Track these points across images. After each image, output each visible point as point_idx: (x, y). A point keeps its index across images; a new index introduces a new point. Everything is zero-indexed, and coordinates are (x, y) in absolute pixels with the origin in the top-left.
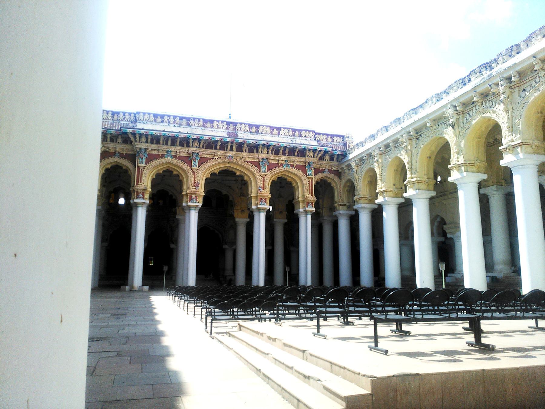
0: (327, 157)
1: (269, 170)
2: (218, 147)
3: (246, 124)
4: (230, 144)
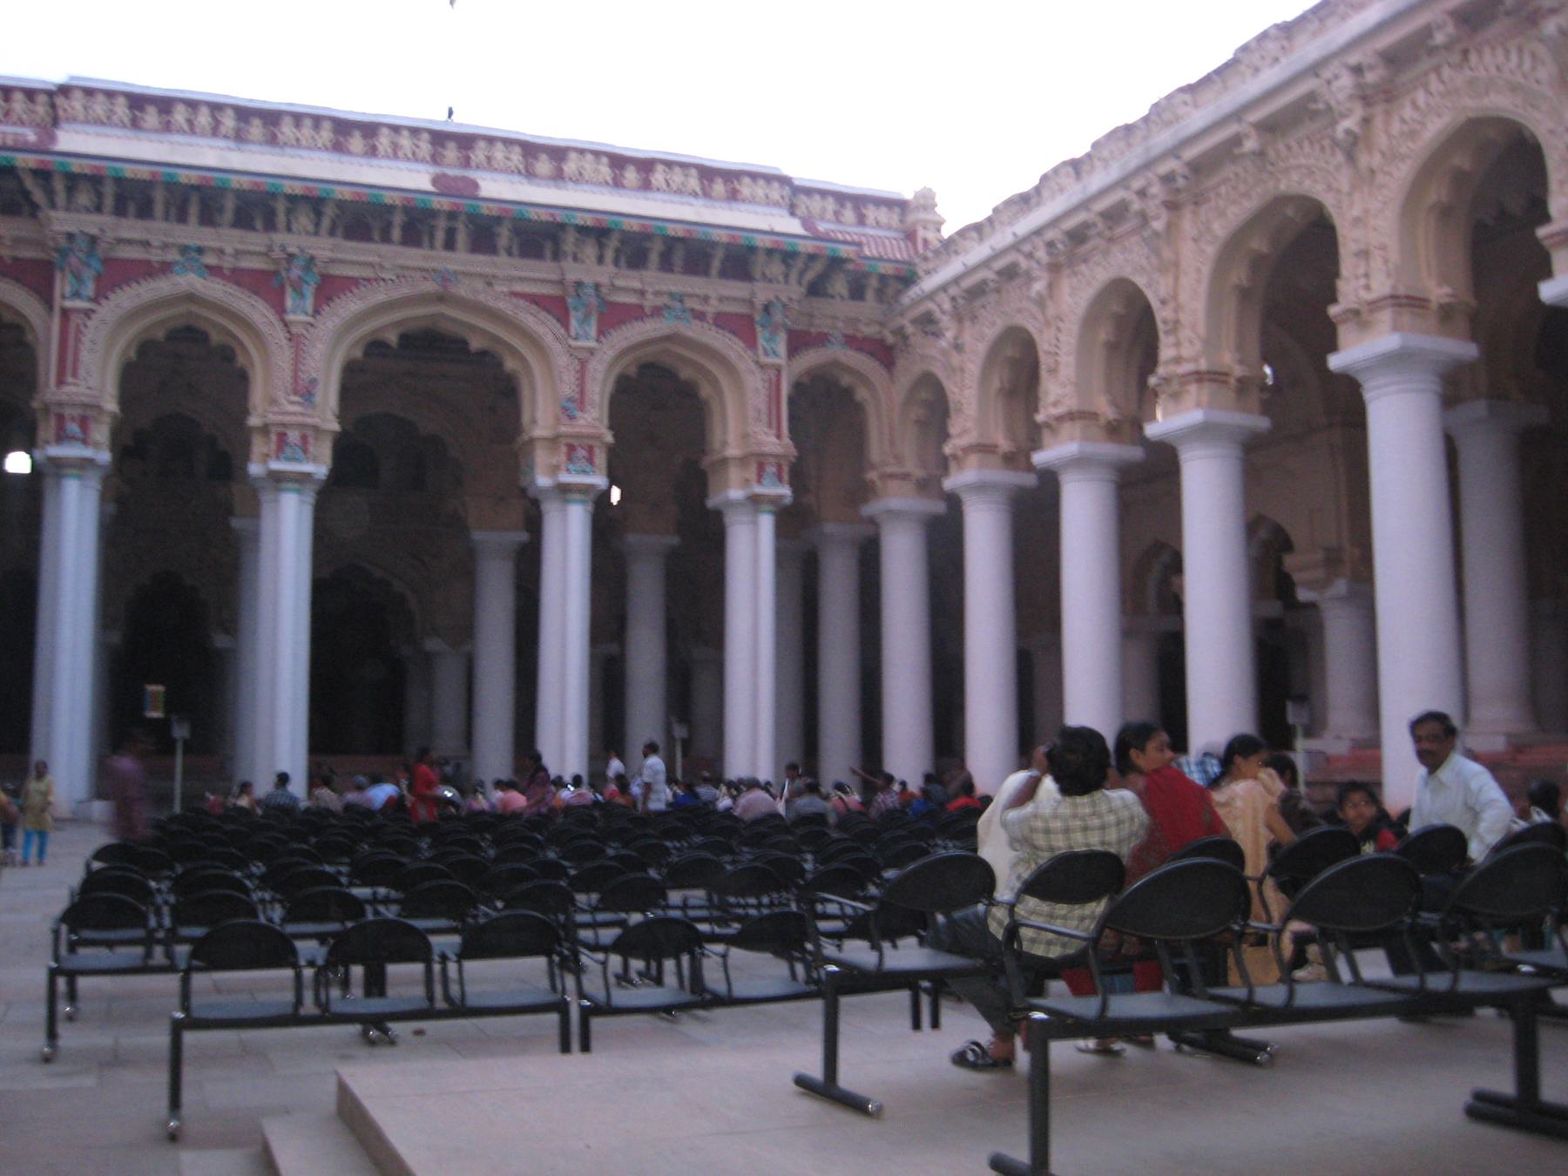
0: (839, 286)
2: (396, 233)
4: (442, 224)
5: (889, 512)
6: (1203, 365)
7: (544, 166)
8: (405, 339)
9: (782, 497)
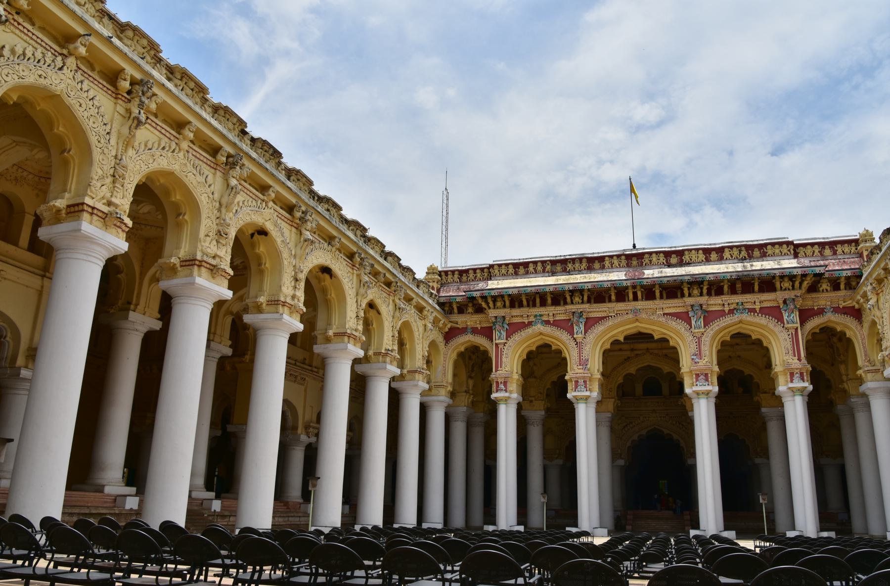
0: (825, 286)
1: (706, 324)
2: (613, 297)
3: (660, 252)
5: (868, 389)
8: (626, 338)
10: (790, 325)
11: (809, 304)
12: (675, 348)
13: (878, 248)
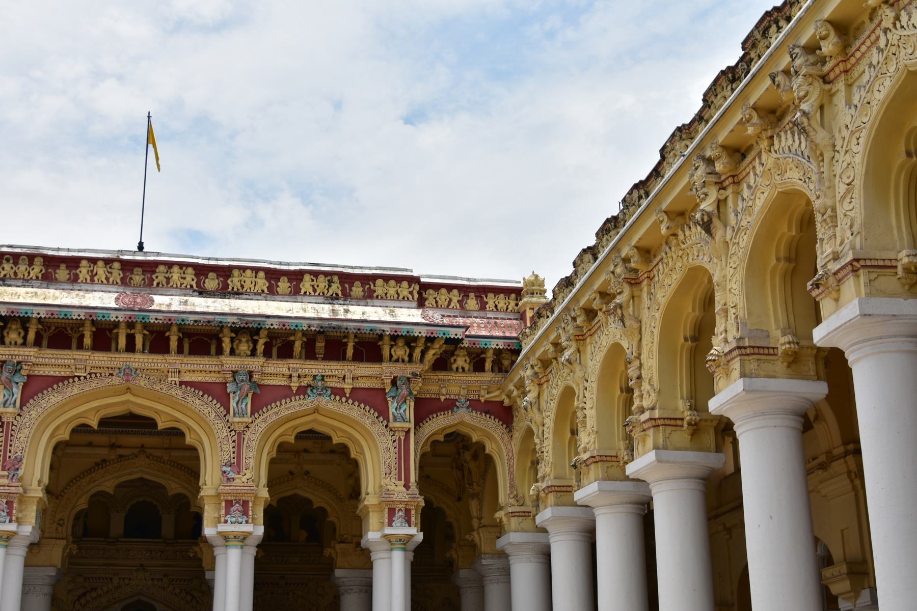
0: (461, 361)
2: (87, 341)
3: (188, 265)
5: (510, 544)
6: (657, 414)
7: (211, 283)
8: (103, 422)
9: (412, 536)
10: (398, 425)
11: (432, 390)
12: (194, 449)
13: (550, 307)
